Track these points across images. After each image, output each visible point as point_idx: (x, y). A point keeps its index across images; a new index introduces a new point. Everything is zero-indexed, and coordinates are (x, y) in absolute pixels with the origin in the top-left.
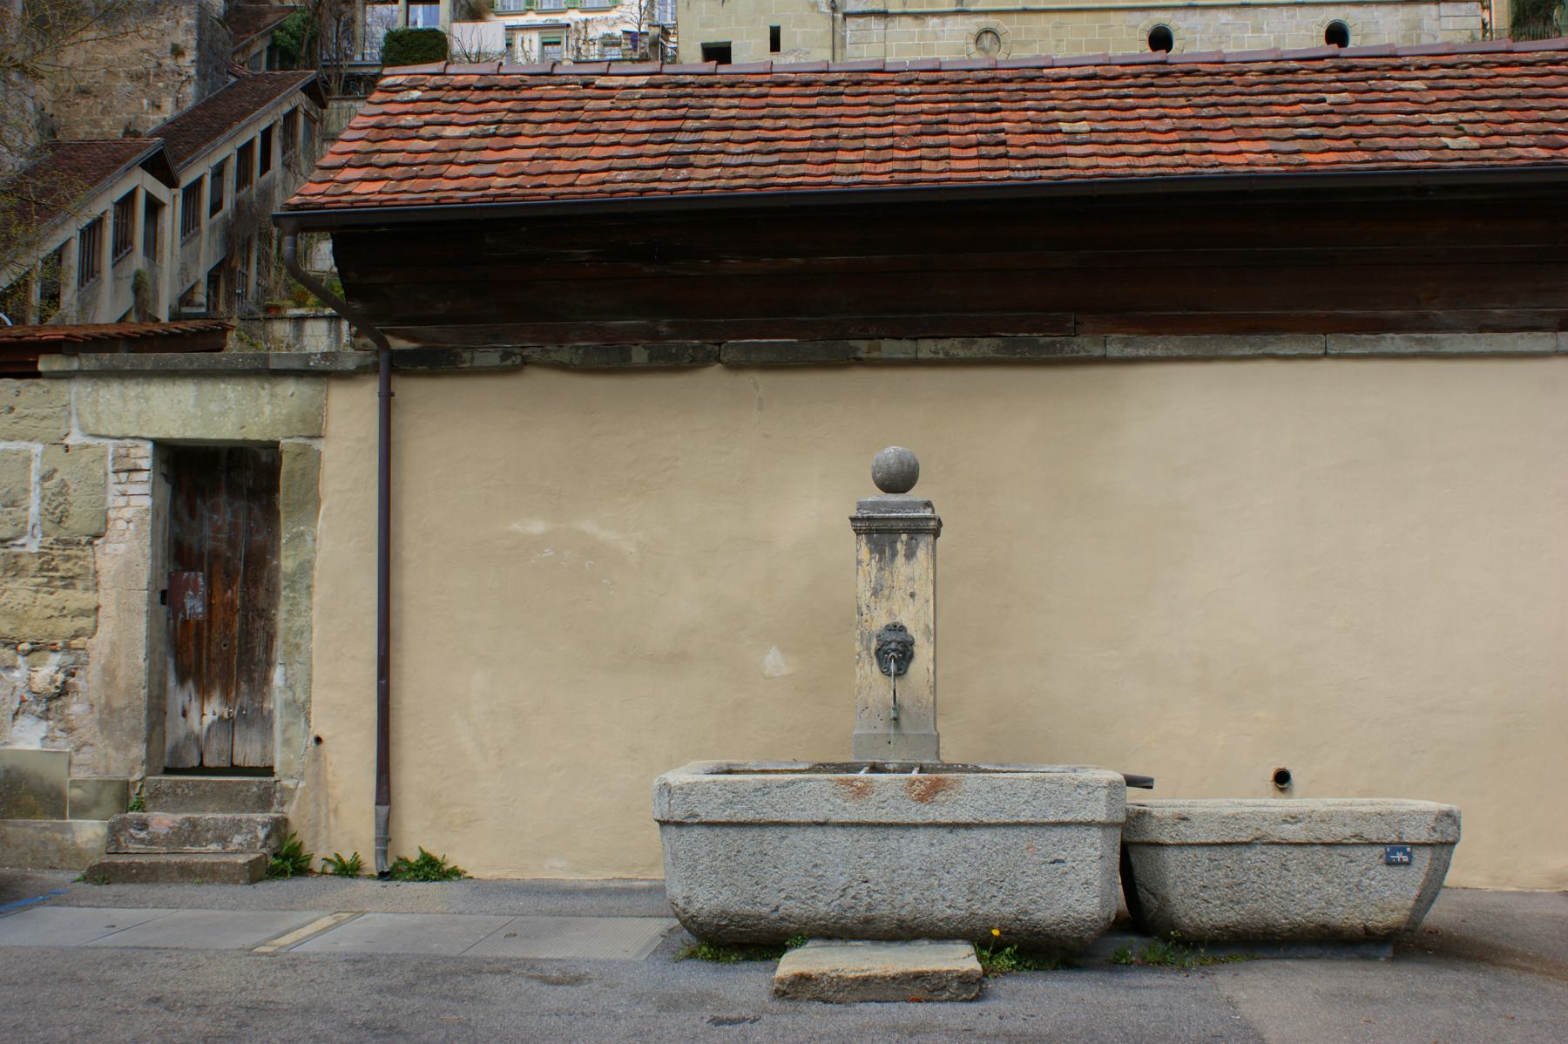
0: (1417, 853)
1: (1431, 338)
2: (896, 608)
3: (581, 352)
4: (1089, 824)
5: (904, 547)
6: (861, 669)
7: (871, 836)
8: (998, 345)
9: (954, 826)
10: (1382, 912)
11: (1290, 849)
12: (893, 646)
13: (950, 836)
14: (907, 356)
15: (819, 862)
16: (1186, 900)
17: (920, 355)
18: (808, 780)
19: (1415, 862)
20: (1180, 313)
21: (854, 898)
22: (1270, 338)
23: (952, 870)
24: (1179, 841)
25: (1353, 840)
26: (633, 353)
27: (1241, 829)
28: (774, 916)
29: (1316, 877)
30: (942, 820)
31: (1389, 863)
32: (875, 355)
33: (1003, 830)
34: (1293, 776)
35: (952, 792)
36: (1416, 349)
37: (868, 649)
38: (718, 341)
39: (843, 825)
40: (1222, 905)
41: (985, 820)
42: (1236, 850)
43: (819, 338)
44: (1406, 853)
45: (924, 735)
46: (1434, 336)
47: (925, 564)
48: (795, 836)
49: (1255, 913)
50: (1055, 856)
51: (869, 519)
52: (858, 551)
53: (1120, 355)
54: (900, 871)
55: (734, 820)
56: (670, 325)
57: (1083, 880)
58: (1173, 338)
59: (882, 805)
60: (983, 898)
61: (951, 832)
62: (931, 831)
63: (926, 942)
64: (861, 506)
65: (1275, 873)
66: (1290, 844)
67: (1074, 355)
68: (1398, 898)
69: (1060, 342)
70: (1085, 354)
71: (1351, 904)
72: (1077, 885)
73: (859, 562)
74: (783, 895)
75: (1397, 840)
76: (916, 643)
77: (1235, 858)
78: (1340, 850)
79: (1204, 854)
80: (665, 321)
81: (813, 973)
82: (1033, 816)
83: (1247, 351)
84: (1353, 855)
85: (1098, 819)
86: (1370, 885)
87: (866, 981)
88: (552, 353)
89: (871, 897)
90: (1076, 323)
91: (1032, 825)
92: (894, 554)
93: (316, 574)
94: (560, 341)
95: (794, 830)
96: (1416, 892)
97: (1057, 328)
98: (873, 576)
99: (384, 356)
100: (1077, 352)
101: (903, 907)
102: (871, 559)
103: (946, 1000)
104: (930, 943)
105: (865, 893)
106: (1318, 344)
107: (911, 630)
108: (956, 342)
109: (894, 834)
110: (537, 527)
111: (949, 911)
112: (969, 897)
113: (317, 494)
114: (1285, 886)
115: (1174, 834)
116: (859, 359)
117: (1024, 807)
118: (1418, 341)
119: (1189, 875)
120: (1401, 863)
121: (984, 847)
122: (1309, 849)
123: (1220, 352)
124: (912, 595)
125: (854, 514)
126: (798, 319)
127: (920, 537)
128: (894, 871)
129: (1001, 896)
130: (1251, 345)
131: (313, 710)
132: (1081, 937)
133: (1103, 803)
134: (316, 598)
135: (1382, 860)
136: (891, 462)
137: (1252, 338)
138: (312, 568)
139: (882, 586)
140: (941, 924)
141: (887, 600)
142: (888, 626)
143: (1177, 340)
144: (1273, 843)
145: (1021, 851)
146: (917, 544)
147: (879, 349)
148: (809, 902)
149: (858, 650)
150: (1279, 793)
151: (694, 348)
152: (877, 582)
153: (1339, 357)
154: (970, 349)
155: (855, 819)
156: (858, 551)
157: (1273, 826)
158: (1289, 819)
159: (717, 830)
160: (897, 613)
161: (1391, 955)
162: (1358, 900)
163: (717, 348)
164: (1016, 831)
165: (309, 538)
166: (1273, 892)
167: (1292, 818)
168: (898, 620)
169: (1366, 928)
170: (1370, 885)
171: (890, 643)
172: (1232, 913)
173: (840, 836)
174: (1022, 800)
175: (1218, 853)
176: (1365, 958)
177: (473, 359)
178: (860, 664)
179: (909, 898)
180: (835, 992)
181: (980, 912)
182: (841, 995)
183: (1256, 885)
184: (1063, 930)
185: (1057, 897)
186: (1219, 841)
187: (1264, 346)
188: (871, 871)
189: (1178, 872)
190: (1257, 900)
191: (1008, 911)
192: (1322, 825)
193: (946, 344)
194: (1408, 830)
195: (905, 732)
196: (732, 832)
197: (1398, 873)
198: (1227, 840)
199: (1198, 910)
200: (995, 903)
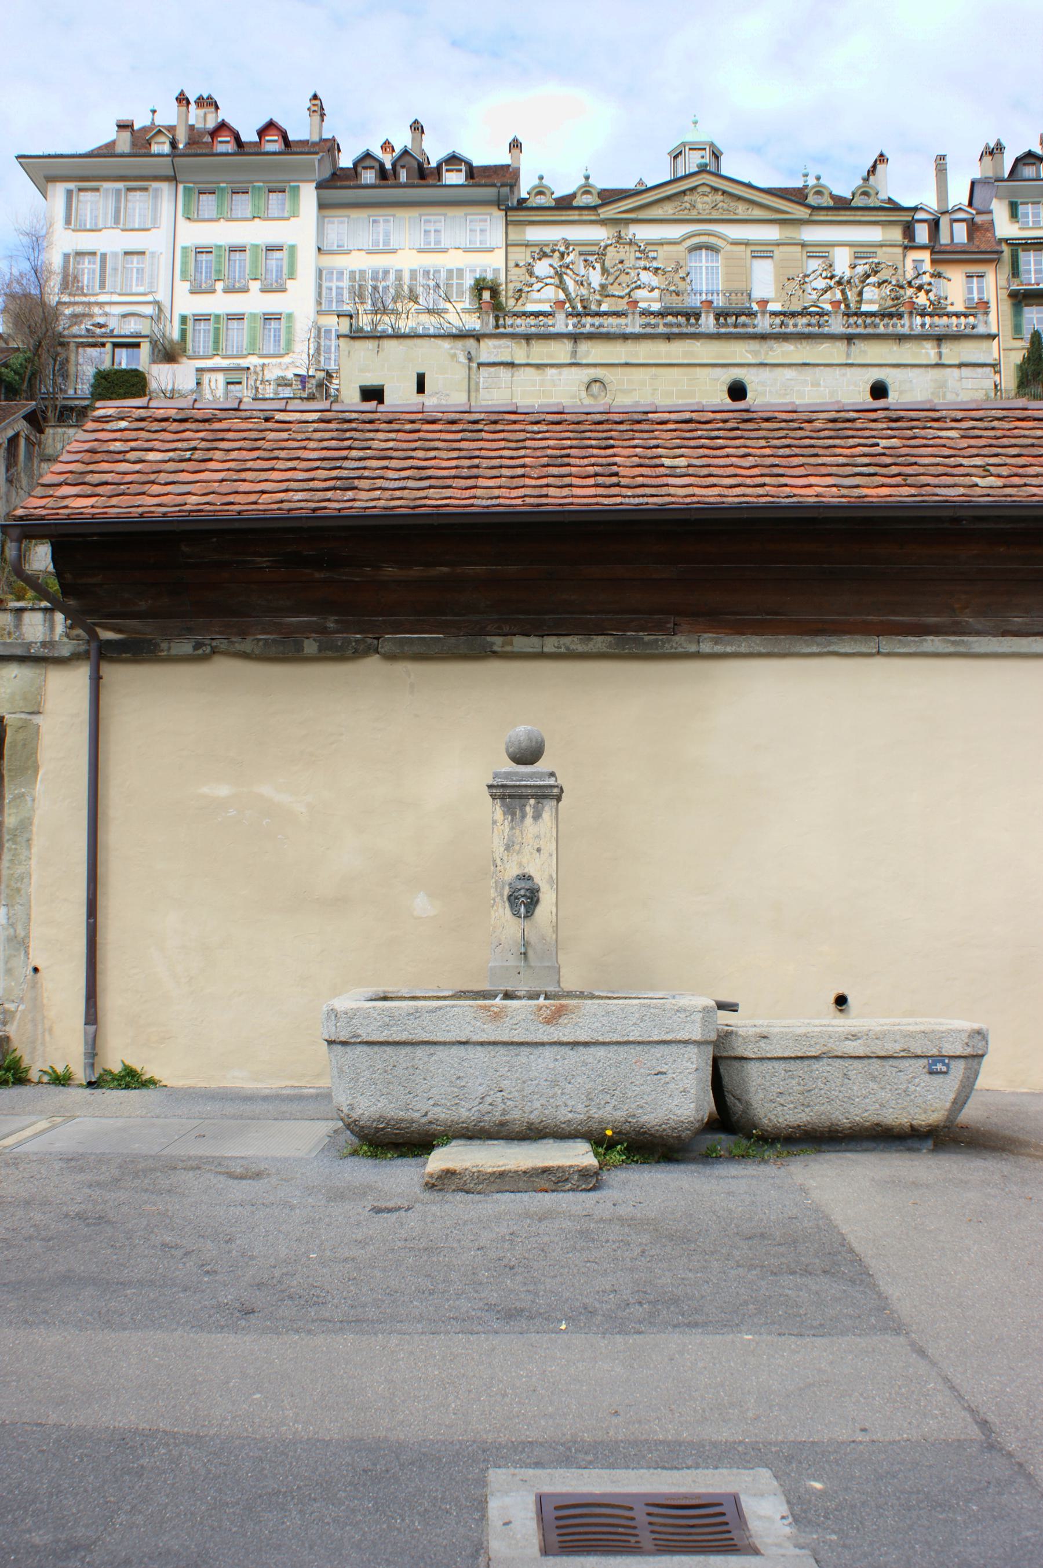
0: (953, 1064)
1: (963, 641)
2: (524, 861)
3: (261, 643)
4: (686, 1042)
6: (497, 911)
7: (505, 1053)
9: (575, 1044)
10: (925, 1113)
11: (850, 1062)
12: (522, 892)
13: (571, 1053)
14: (535, 650)
15: (462, 1075)
16: (766, 1104)
17: (546, 650)
18: (453, 1006)
19: (951, 1071)
20: (760, 617)
21: (491, 1104)
22: (834, 639)
23: (572, 1081)
24: (760, 1056)
25: (902, 1054)
26: (305, 645)
27: (811, 1046)
28: (424, 1120)
29: (872, 1085)
30: (565, 1039)
31: (931, 1073)
32: (508, 648)
33: (616, 1048)
34: (849, 999)
35: (573, 1016)
36: (952, 649)
37: (502, 895)
38: (377, 636)
39: (482, 1044)
40: (795, 1108)
41: (601, 1039)
42: (806, 1062)
43: (462, 634)
44: (944, 1064)
45: (548, 967)
46: (965, 638)
47: (549, 824)
48: (441, 1053)
49: (822, 1114)
50: (659, 1069)
51: (503, 786)
52: (493, 812)
53: (711, 651)
54: (530, 1082)
55: (391, 1040)
56: (336, 622)
57: (682, 1089)
58: (754, 638)
59: (514, 1027)
60: (599, 1104)
61: (572, 1049)
62: (556, 1048)
63: (551, 1141)
64: (496, 775)
65: (838, 1081)
66: (851, 1057)
68: (937, 1101)
69: (662, 640)
71: (900, 1106)
72: (676, 1093)
73: (494, 822)
74: (431, 1102)
75: (937, 1054)
77: (806, 1069)
78: (891, 1062)
79: (780, 1066)
80: (333, 618)
81: (457, 1168)
82: (640, 1036)
83: (815, 649)
84: (901, 1066)
85: (694, 1038)
86: (915, 1090)
87: (502, 1175)
88: (236, 645)
89: (505, 1104)
90: (675, 624)
91: (639, 1043)
92: (524, 816)
93: (35, 829)
94: (243, 634)
95: (441, 1048)
96: (952, 1096)
97: (659, 628)
98: (506, 834)
99: (94, 645)
100: (676, 648)
101: (532, 1112)
103: (569, 1190)
104: (555, 1142)
105: (500, 1100)
106: (872, 644)
107: (537, 880)
108: (575, 638)
109: (526, 1050)
110: (223, 791)
111: (570, 1115)
112: (587, 1104)
113: (36, 761)
114: (847, 1092)
115: (756, 1050)
116: (494, 652)
117: (633, 1028)
118: (953, 643)
119: (768, 1084)
120: (941, 1073)
121: (599, 1061)
122: (866, 1062)
123: (793, 650)
124: (539, 850)
125: (490, 782)
126: (444, 618)
127: (545, 802)
128: (524, 1082)
129: (613, 1102)
130: (818, 645)
131: (32, 944)
132: (680, 1136)
133: (698, 1025)
134: (34, 850)
135: (925, 1070)
136: (522, 738)
137: (819, 639)
138: (31, 824)
139: (513, 842)
140: (563, 1126)
143: (757, 639)
144: (837, 1057)
145: (631, 1065)
146: (543, 807)
147: (511, 644)
148: (453, 1108)
149: (493, 896)
150: (838, 1013)
151: (357, 641)
152: (509, 839)
153: (889, 655)
154: (587, 645)
155: (492, 1039)
156: (493, 812)
157: (837, 1043)
158: (850, 1037)
159: (376, 1048)
160: (526, 865)
161: (931, 1147)
162: (905, 1103)
163: (375, 642)
164: (626, 1048)
165: (28, 799)
166: (837, 1097)
167: (853, 1036)
169: (912, 1126)
170: (915, 1090)
171: (520, 890)
172: (803, 1115)
173: (480, 1052)
174: (631, 1023)
175: (792, 1065)
176: (910, 1150)
177: (169, 648)
178: (495, 908)
179: (537, 1105)
180: (475, 1184)
181: (596, 1116)
182: (481, 1186)
183: (823, 1092)
184: (664, 1130)
185: (660, 1103)
186: (793, 1055)
187: (829, 645)
188: (505, 1082)
189: (759, 1081)
190: (823, 1104)
191: (620, 1115)
192: (877, 1041)
193: (567, 640)
194: (946, 1045)
195: (532, 964)
196: (389, 1050)
197: (938, 1080)
198: (799, 1054)
199: (775, 1112)
200: (609, 1108)
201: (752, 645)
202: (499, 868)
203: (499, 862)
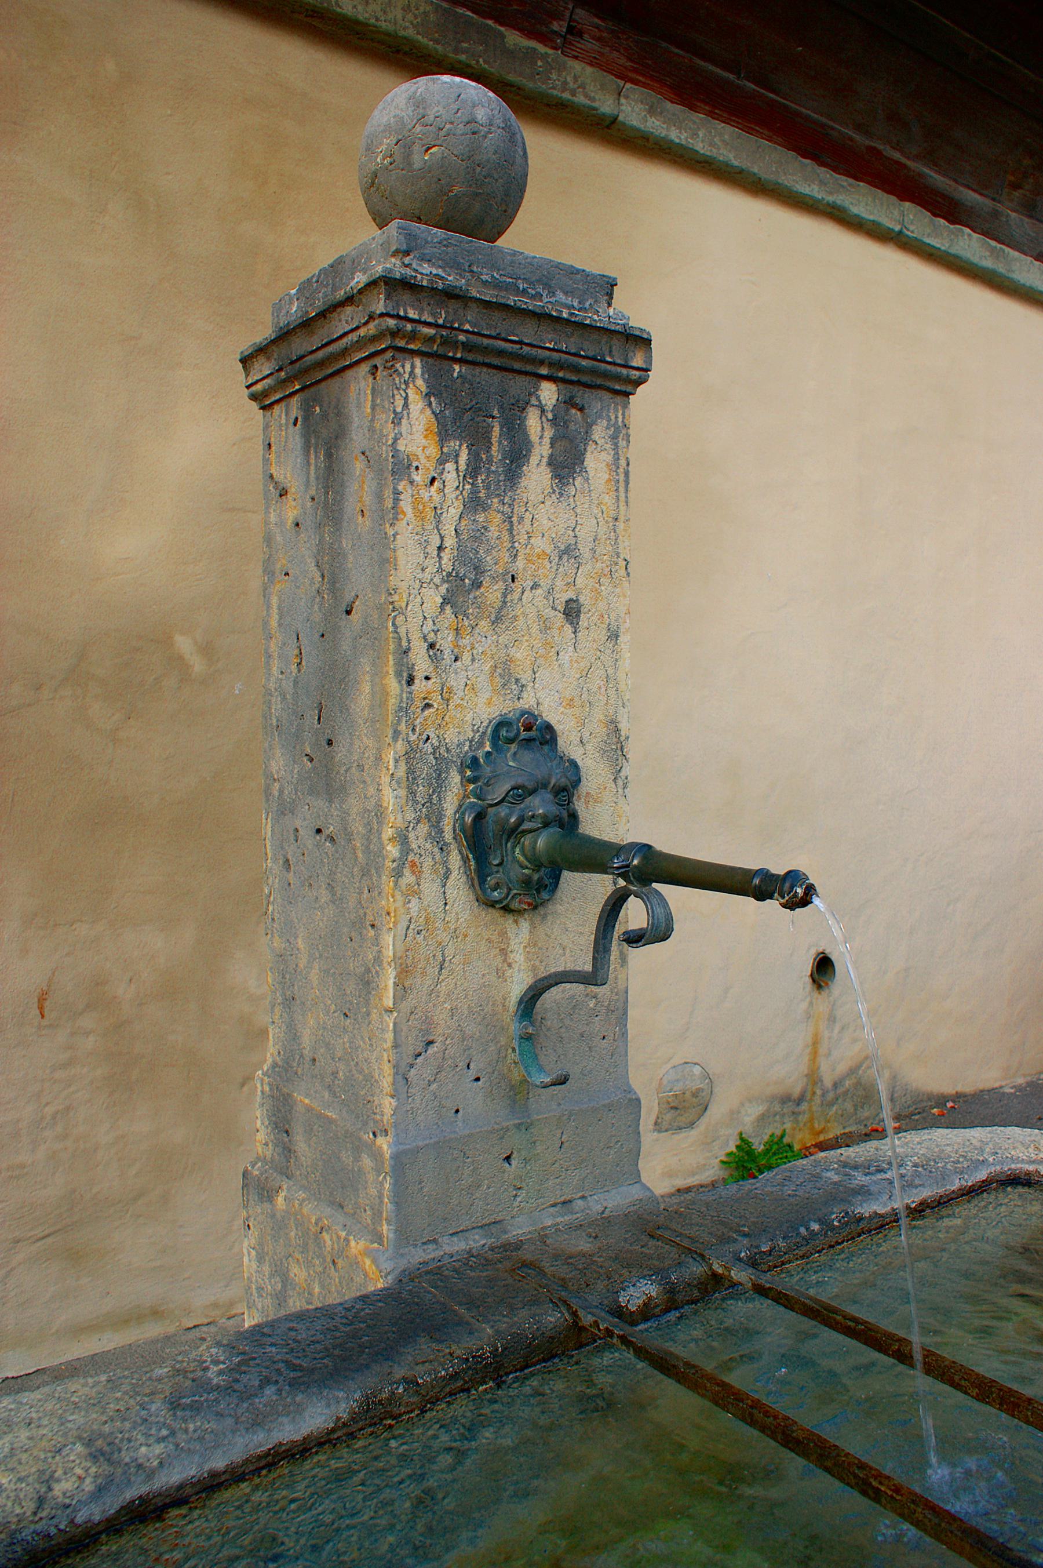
5: (549, 434)
6: (414, 891)
8: (426, 14)
37: (435, 819)
51: (451, 295)
67: (566, 95)
69: (544, 57)
70: (587, 102)
76: (587, 786)
90: (571, 30)
98: (449, 530)
102: (442, 461)
107: (569, 744)
124: (572, 612)
130: (822, 183)
139: (478, 569)
141: (497, 620)
142: (502, 724)
152: (462, 555)
160: (525, 677)
168: (528, 701)
178: (408, 878)
201: (717, 140)
202: (419, 685)
203: (421, 663)
